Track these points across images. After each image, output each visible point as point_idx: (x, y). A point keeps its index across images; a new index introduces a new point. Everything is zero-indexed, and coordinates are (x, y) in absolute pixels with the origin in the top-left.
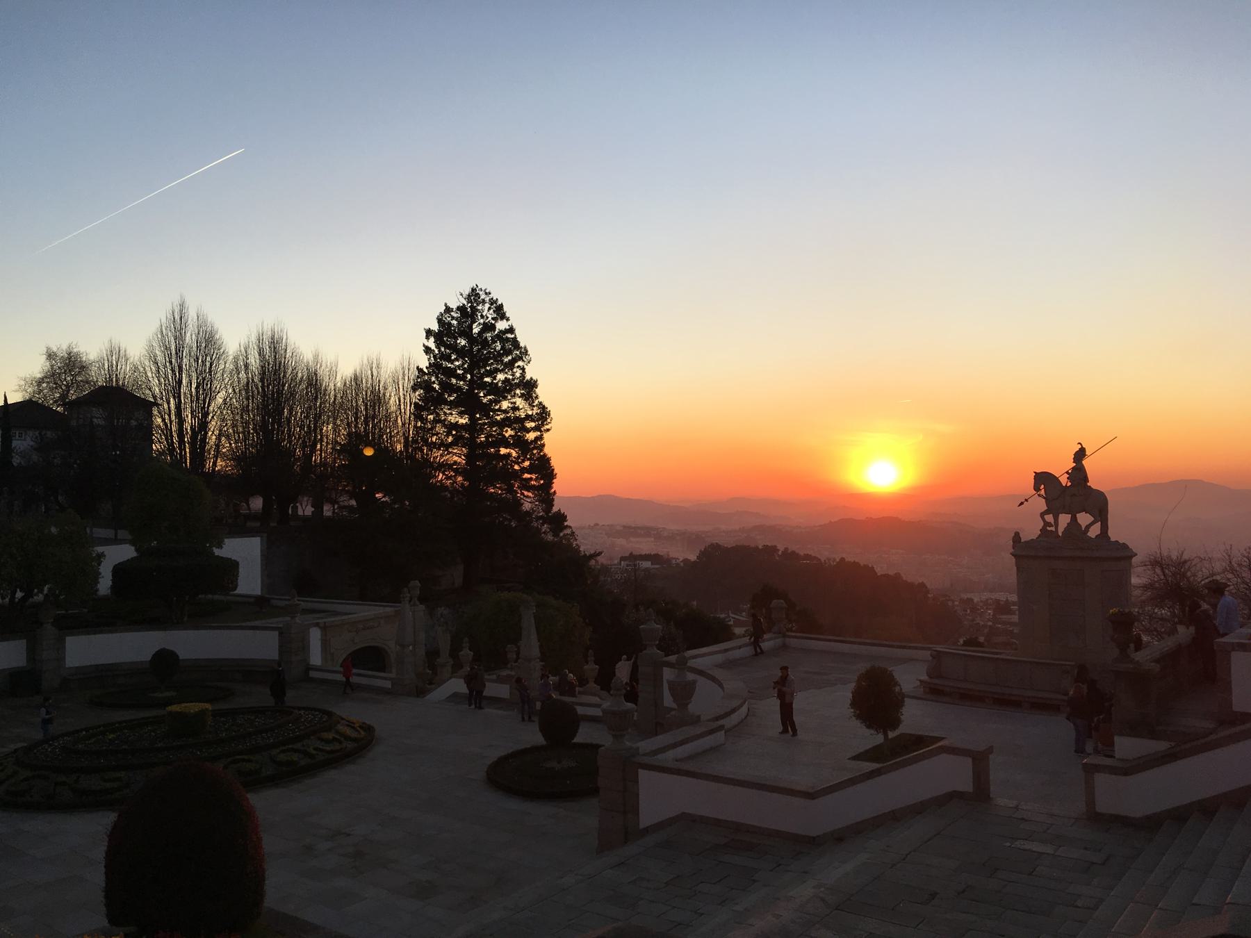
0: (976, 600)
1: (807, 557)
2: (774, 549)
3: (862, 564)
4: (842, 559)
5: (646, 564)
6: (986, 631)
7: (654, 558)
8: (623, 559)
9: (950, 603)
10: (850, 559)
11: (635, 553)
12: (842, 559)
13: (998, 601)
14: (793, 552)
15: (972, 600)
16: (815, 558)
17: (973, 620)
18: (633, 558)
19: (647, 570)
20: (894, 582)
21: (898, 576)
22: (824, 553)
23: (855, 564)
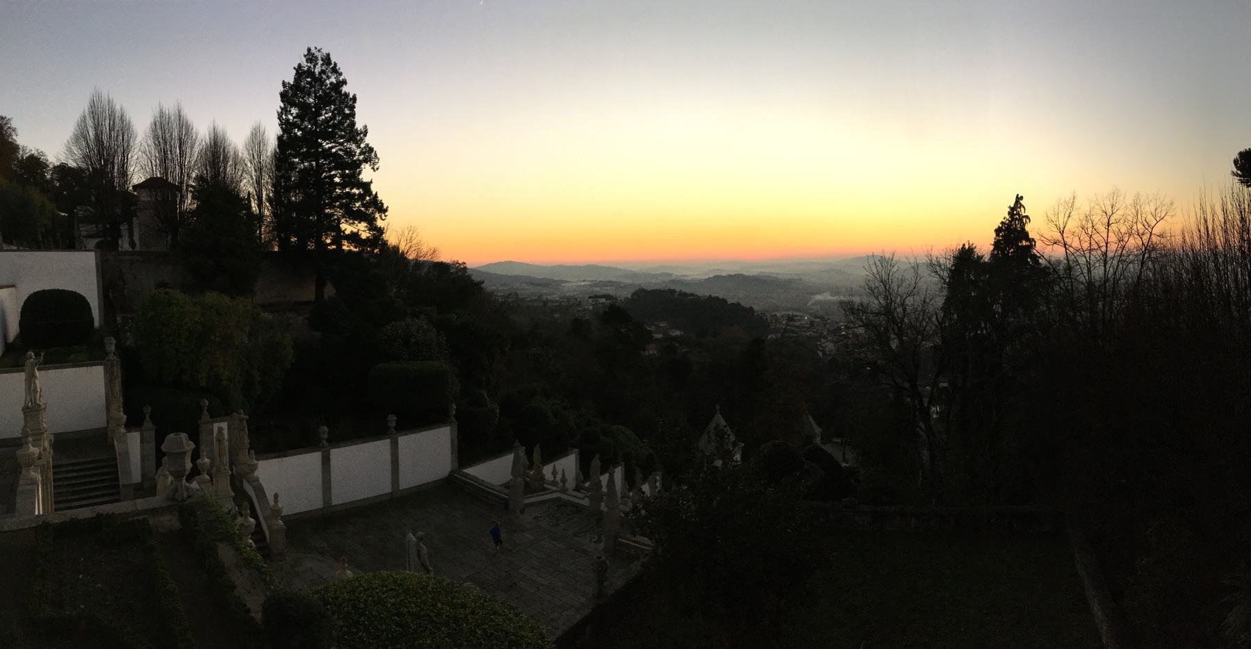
0: (778, 315)
1: (692, 295)
2: (674, 291)
3: (720, 297)
4: (710, 296)
5: (603, 300)
6: (782, 331)
7: (608, 297)
8: (590, 297)
9: (765, 317)
10: (713, 295)
11: (598, 294)
12: (710, 296)
13: (789, 315)
14: (685, 292)
15: (776, 315)
16: (697, 295)
17: (776, 325)
18: (596, 297)
19: (603, 303)
20: (737, 306)
21: (739, 304)
22: (703, 292)
23: (717, 298)
